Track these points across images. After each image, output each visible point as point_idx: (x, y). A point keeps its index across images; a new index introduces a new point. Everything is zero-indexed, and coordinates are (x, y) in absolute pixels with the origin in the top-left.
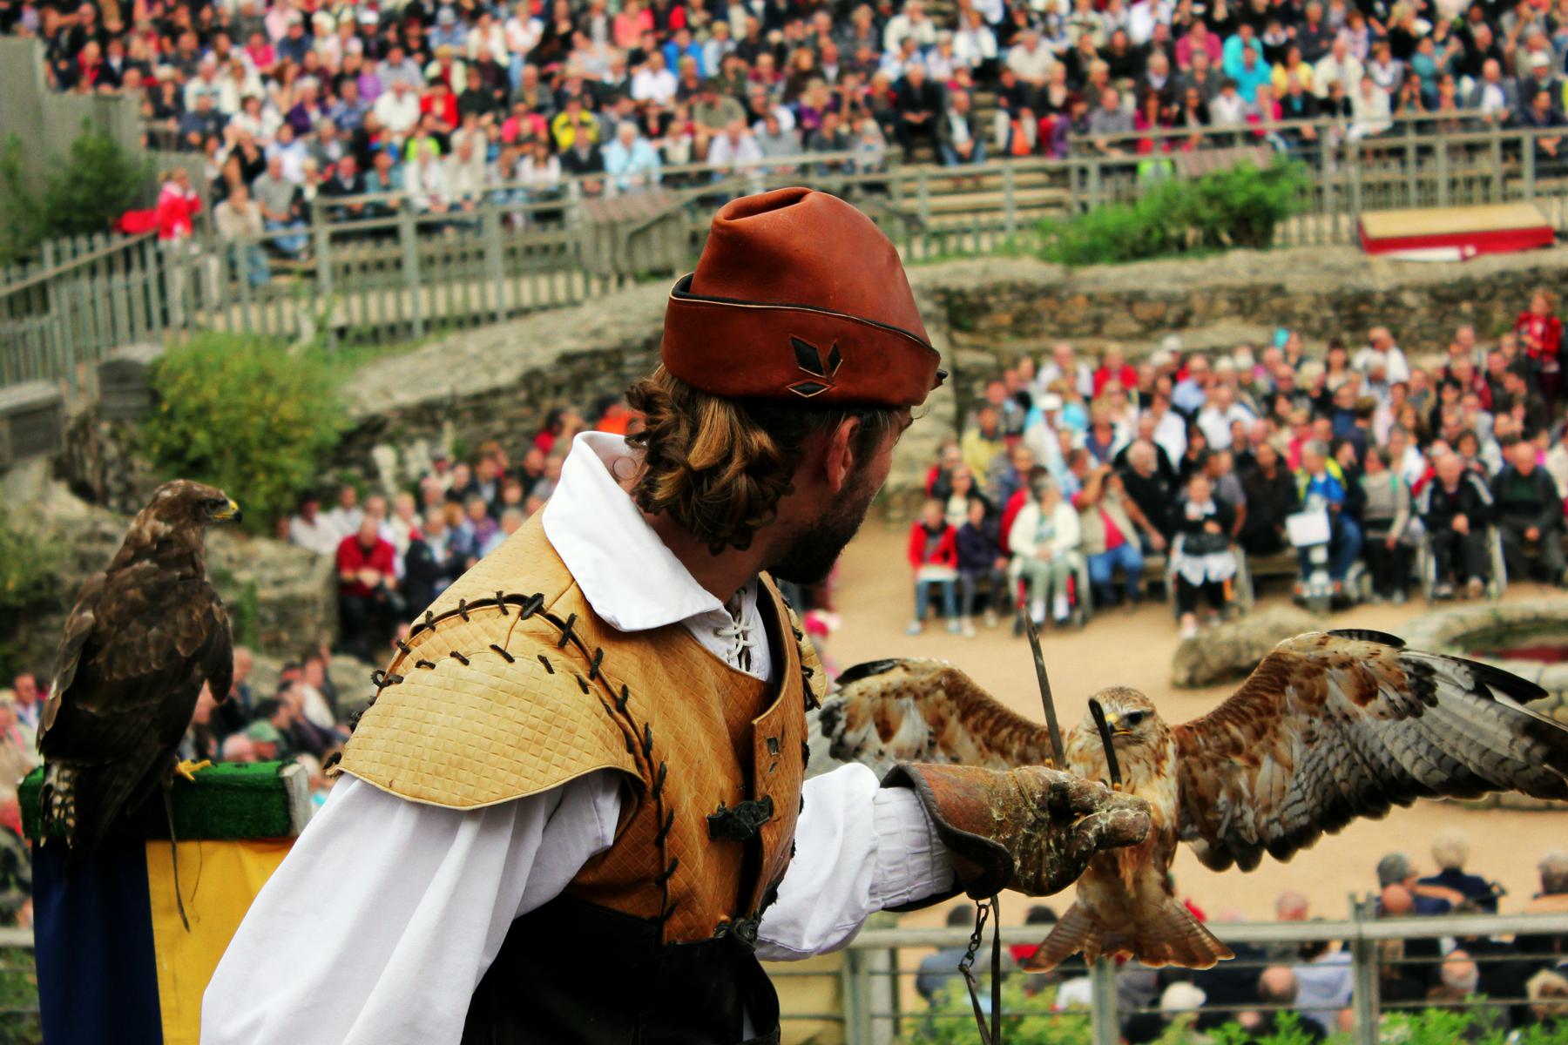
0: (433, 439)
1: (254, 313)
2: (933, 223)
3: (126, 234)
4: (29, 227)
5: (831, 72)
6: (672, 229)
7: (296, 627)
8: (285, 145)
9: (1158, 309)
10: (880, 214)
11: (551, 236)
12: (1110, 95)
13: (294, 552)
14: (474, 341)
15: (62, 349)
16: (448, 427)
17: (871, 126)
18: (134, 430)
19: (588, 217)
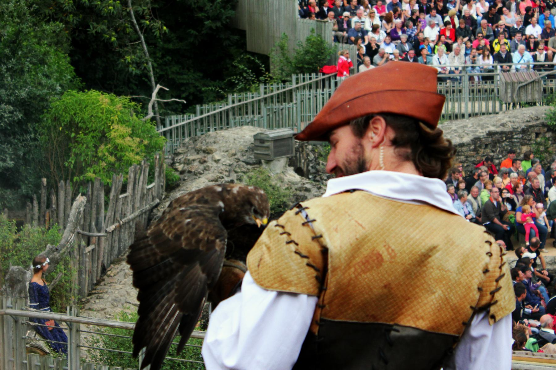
4: (287, 69)
6: (536, 86)
8: (388, 44)
11: (488, 86)
15: (296, 117)
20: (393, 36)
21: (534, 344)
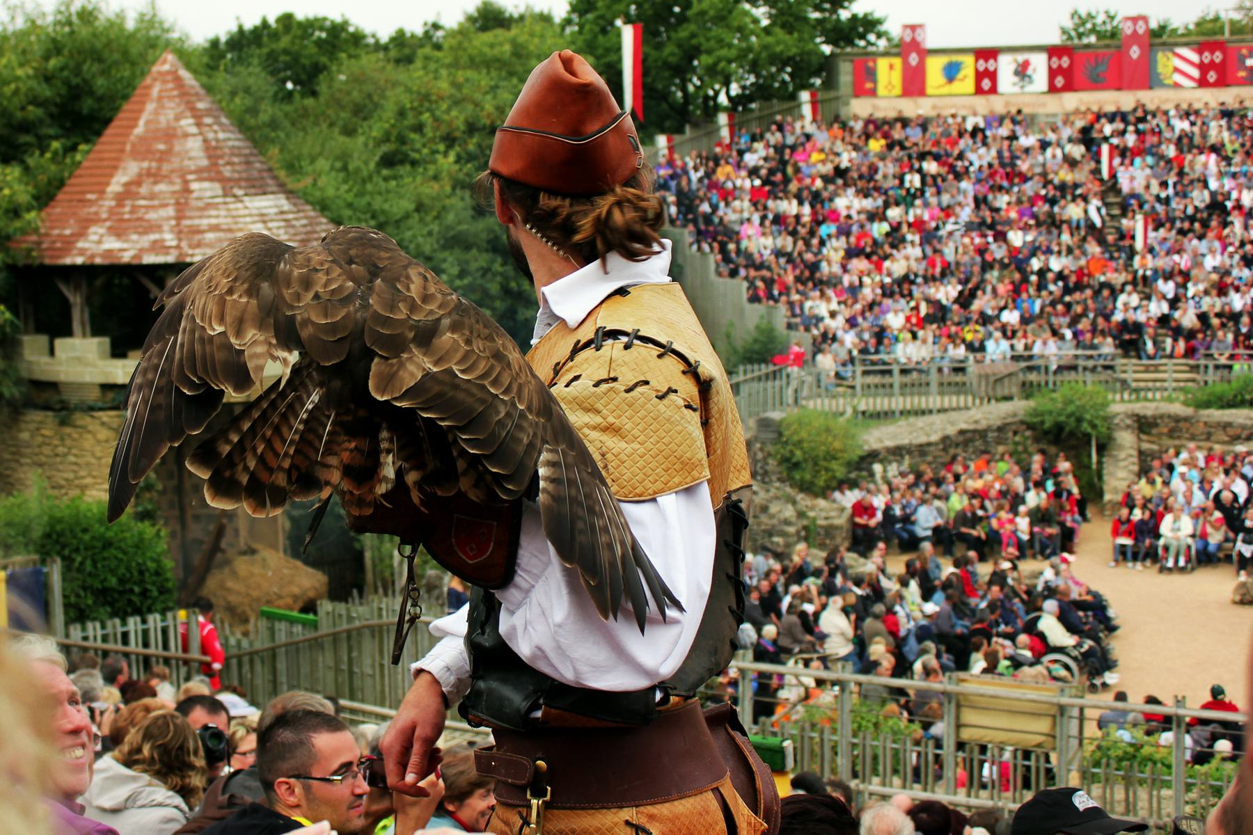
0: (900, 462)
1: (827, 401)
2: (1134, 385)
3: (775, 365)
4: (734, 359)
5: (1091, 315)
6: (1014, 379)
7: (833, 538)
8: (846, 332)
9: (1238, 431)
10: (1109, 379)
11: (959, 378)
12: (1220, 334)
13: (835, 506)
14: (921, 422)
16: (907, 457)
17: (1109, 340)
18: (770, 448)
19: (976, 371)
20: (852, 322)
21: (1008, 667)
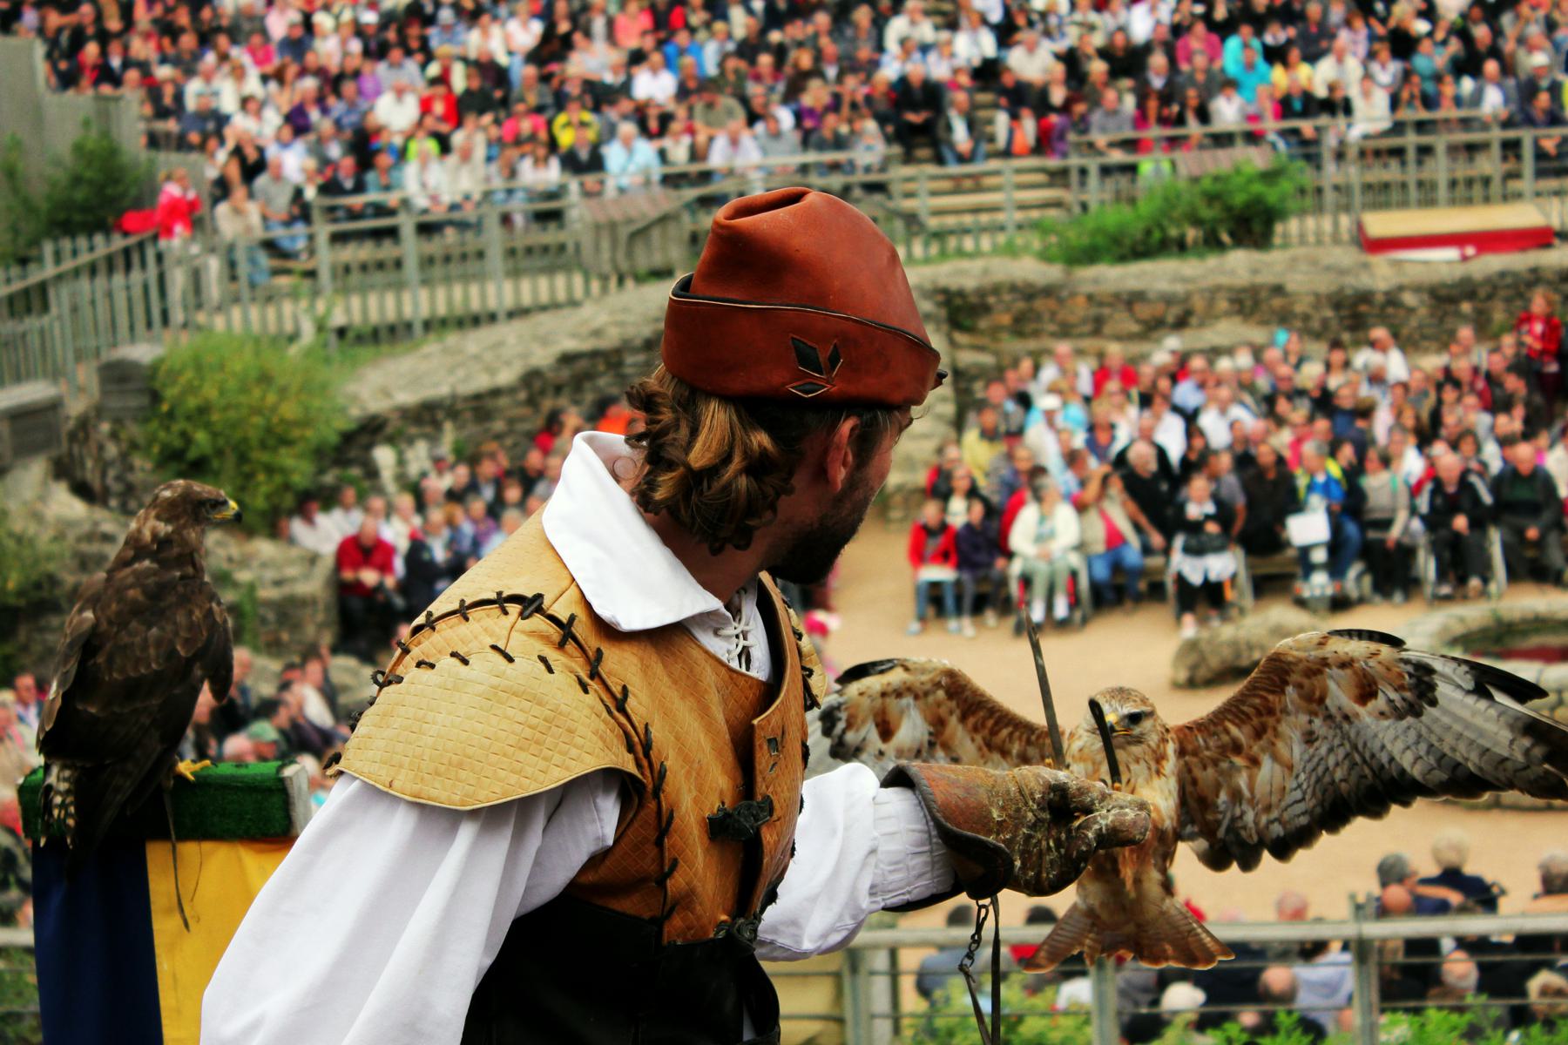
6: (672, 229)
11: (551, 236)
